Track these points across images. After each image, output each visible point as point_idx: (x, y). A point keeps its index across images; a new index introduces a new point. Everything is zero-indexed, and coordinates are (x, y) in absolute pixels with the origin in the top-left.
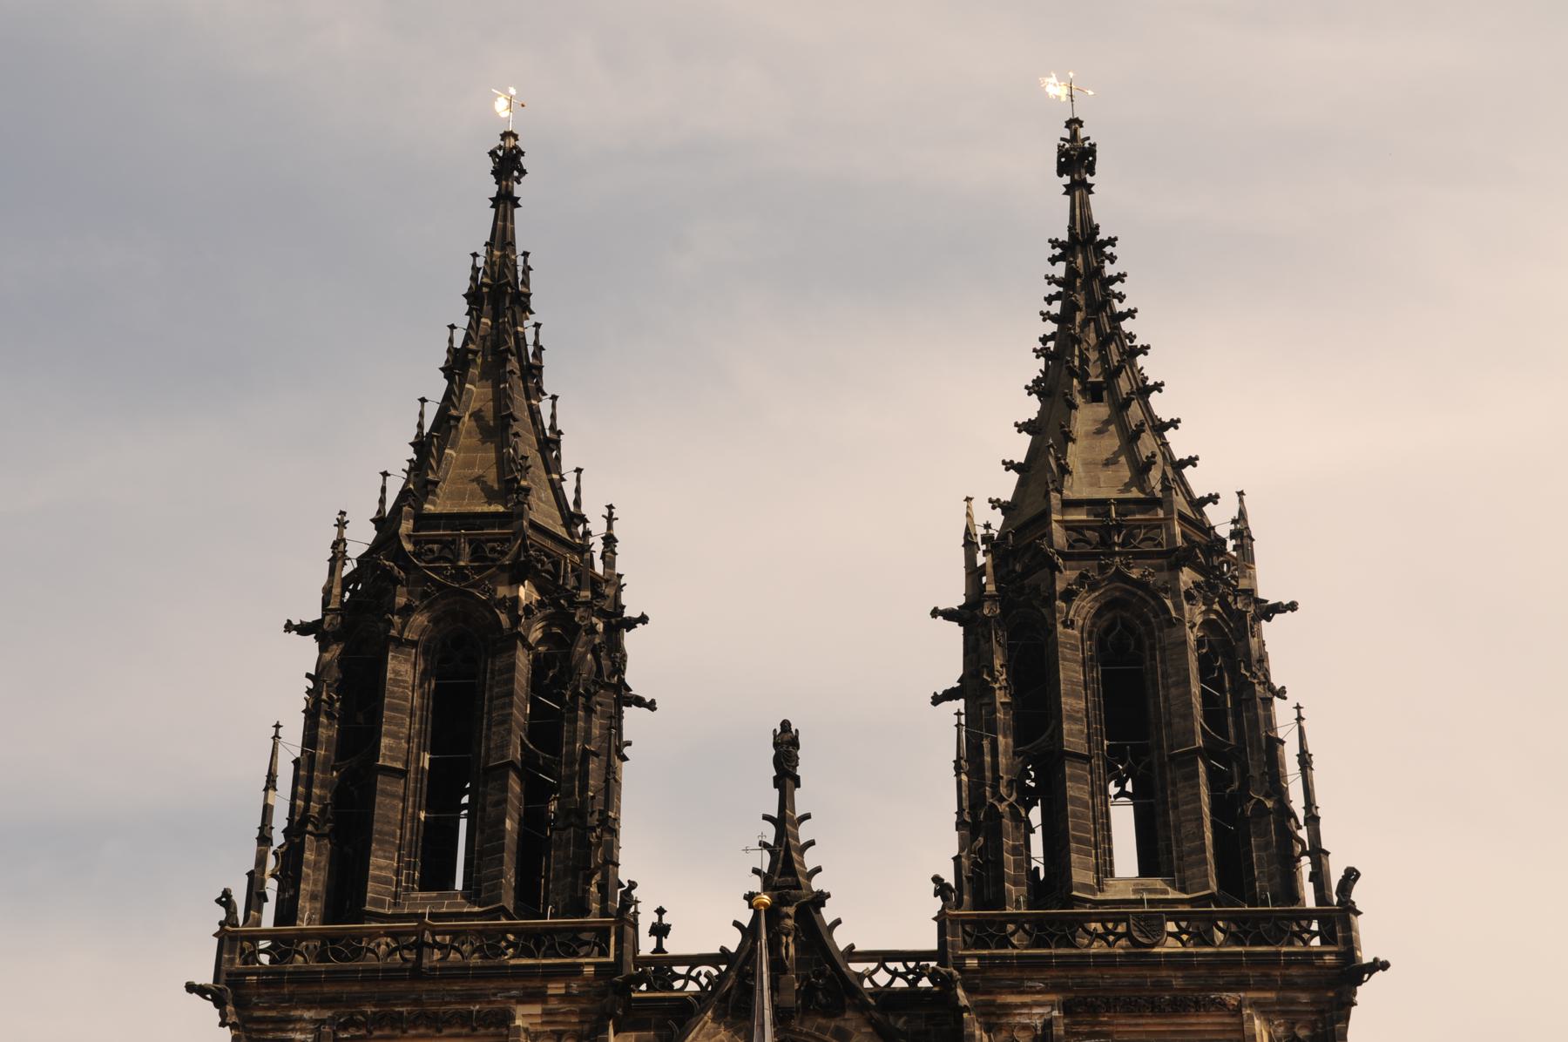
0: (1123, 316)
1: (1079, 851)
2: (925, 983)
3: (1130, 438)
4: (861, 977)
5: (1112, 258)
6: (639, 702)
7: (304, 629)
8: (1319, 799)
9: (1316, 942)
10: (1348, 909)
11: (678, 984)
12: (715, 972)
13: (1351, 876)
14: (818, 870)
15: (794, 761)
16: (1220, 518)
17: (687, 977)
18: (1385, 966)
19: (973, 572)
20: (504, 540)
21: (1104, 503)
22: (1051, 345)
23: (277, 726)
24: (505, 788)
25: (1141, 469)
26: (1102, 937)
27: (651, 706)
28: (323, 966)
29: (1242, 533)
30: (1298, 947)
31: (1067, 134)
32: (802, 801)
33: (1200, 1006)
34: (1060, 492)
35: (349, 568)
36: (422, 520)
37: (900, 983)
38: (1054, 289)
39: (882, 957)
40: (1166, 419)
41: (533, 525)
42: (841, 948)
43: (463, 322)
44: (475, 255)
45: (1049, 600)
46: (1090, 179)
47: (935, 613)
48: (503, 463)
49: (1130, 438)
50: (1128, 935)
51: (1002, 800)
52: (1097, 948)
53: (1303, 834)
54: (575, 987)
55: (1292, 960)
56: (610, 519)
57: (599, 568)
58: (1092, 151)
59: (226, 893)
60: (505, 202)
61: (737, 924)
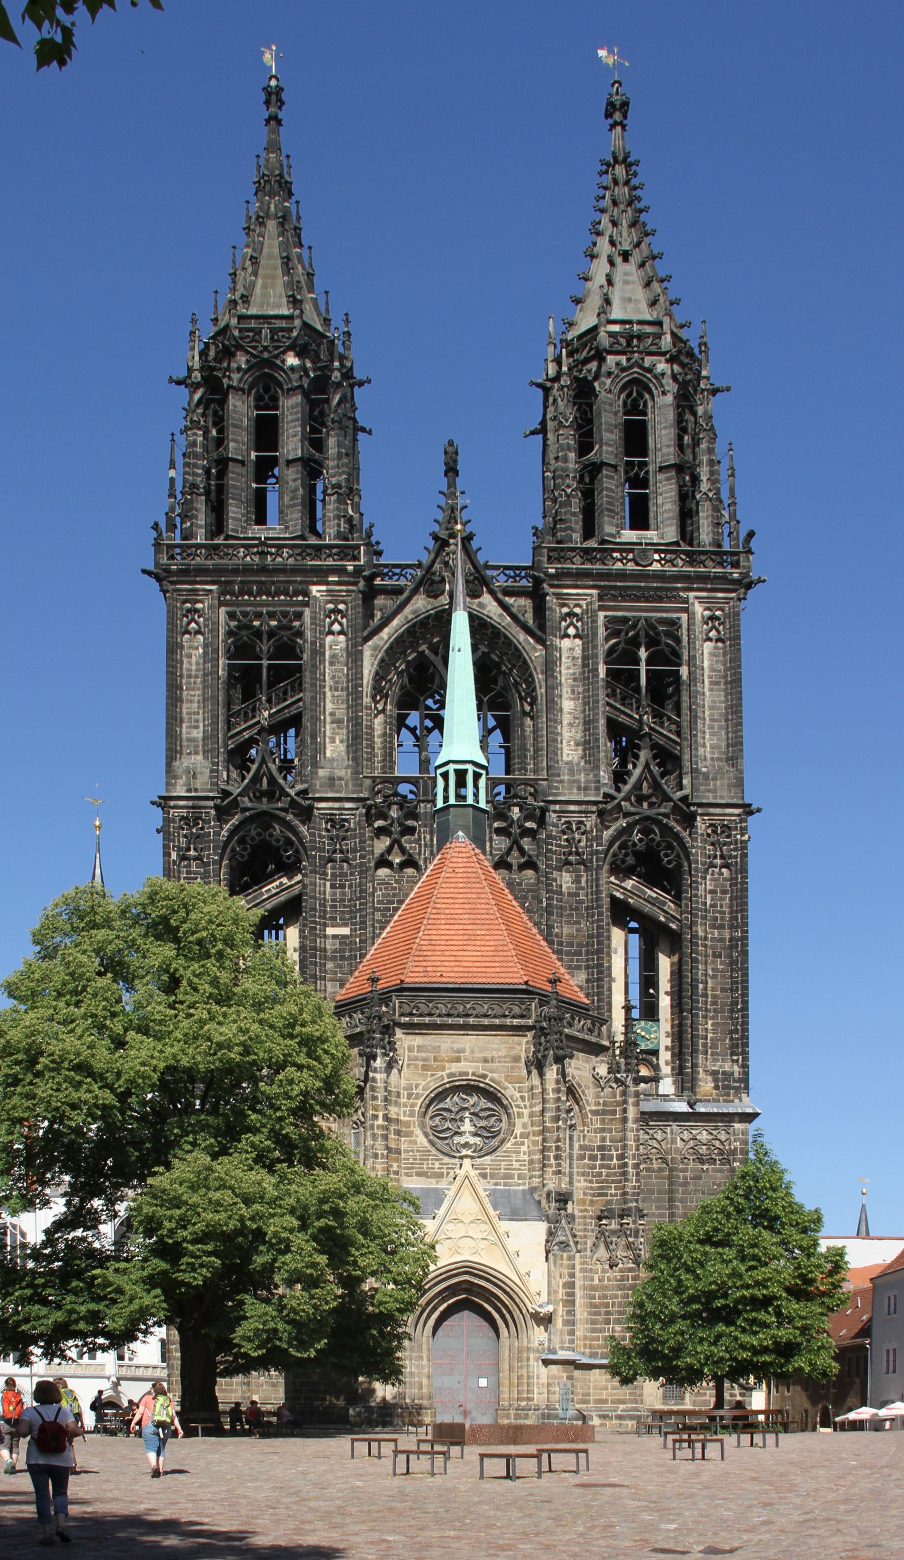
15: (455, 461)
44: (258, 156)
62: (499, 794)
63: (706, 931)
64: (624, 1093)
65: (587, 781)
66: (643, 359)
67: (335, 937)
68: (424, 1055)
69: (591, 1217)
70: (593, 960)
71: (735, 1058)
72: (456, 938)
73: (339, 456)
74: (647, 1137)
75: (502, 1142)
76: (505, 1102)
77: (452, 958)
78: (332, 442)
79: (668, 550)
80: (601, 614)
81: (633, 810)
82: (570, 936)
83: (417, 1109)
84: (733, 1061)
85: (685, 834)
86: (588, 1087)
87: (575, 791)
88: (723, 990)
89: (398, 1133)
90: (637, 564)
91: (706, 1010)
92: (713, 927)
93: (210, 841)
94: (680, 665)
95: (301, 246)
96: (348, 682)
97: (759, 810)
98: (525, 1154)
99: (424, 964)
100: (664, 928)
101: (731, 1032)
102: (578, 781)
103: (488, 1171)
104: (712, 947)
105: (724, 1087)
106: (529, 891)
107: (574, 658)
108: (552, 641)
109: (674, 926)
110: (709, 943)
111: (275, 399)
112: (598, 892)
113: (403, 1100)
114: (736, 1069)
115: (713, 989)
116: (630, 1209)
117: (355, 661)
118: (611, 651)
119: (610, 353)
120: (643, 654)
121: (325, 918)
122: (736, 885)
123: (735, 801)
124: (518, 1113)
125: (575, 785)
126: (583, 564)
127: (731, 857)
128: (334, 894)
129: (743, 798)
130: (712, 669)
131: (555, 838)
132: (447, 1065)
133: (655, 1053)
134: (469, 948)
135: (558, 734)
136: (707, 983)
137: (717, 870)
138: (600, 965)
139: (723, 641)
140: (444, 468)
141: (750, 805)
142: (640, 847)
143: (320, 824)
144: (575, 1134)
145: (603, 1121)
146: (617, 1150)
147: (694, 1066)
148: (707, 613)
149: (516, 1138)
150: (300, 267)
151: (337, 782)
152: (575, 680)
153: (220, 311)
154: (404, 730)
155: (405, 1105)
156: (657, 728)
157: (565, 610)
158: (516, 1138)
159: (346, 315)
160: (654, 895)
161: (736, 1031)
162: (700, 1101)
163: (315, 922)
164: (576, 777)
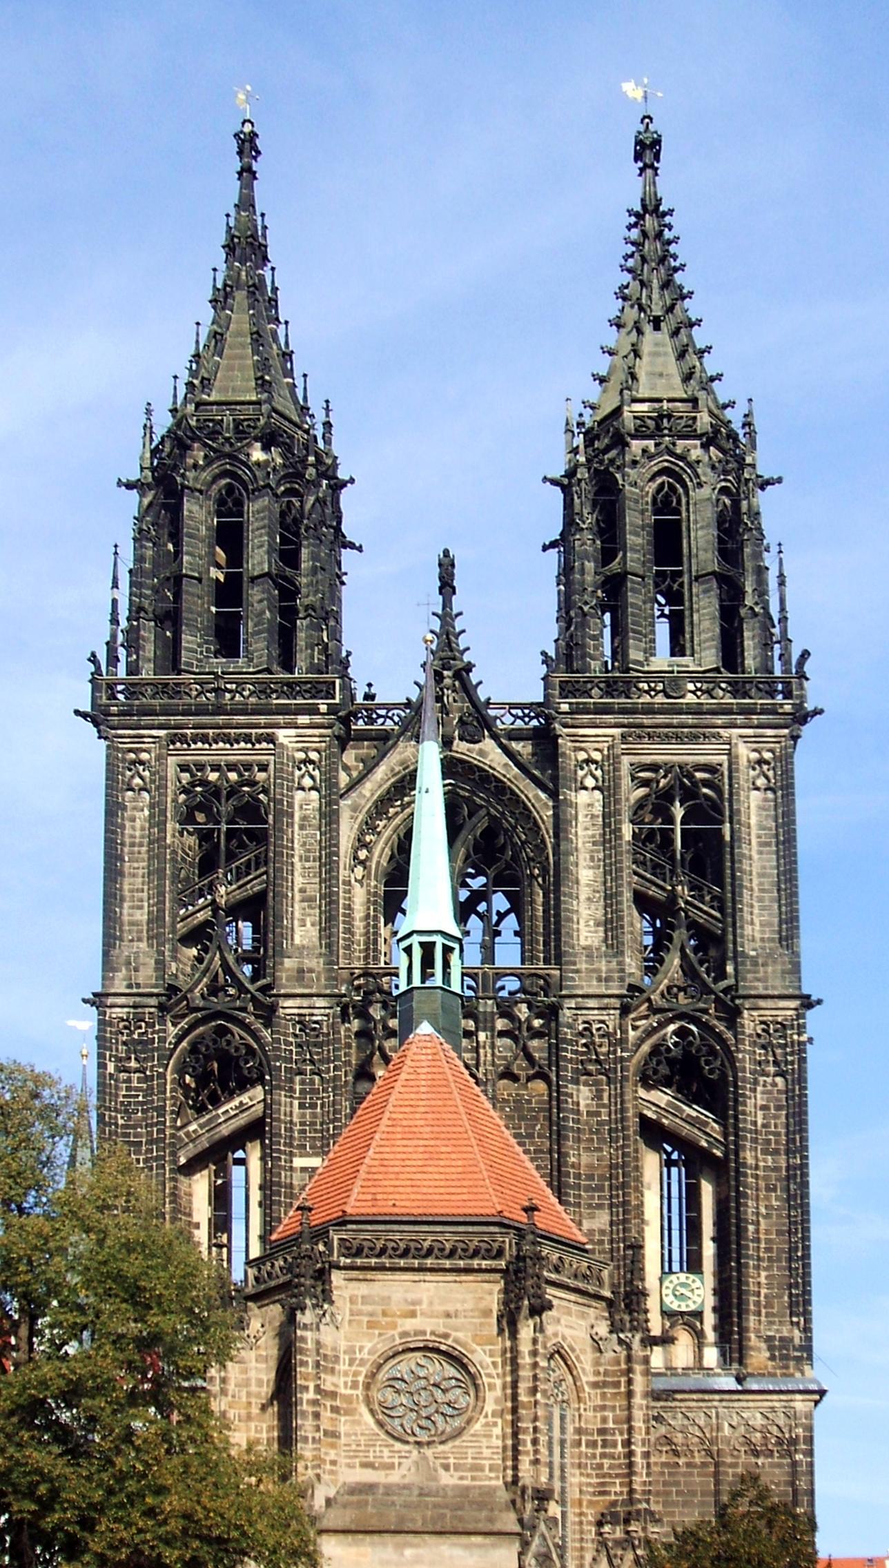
1: (634, 639)
5: (670, 227)
9: (780, 696)
11: (380, 721)
12: (403, 714)
14: (468, 649)
16: (735, 417)
17: (386, 717)
23: (116, 546)
26: (647, 692)
32: (457, 603)
42: (483, 699)
47: (545, 479)
50: (663, 691)
51: (586, 603)
54: (318, 719)
62: (503, 988)
63: (757, 1158)
64: (629, 1359)
65: (609, 971)
66: (674, 444)
67: (304, 1169)
68: (369, 1308)
69: (589, 1523)
70: (618, 1196)
71: (795, 1319)
72: (415, 1156)
73: (314, 571)
74: (686, 1422)
75: (469, 1422)
76: (472, 1370)
77: (409, 1183)
78: (304, 553)
79: (707, 680)
80: (626, 760)
82: (590, 1166)
83: (361, 1379)
84: (792, 1323)
85: (729, 1035)
86: (583, 1351)
87: (595, 983)
88: (779, 1233)
89: (335, 1410)
90: (668, 697)
91: (759, 1259)
92: (765, 1152)
93: (153, 1050)
94: (722, 822)
95: (277, 320)
96: (321, 850)
97: (819, 1002)
99: (373, 1190)
100: (706, 1155)
101: (790, 1286)
102: (598, 971)
104: (766, 1178)
105: (783, 1357)
106: (541, 1110)
107: (593, 816)
108: (564, 794)
109: (719, 1153)
110: (761, 1173)
111: (239, 503)
112: (623, 1110)
113: (342, 1367)
114: (797, 1334)
115: (767, 1232)
116: (638, 1511)
117: (329, 824)
118: (640, 805)
119: (634, 437)
120: (678, 811)
121: (291, 1145)
122: (793, 1097)
123: (791, 991)
124: (489, 1385)
125: (595, 975)
126: (601, 697)
128: (303, 1115)
129: (800, 988)
130: (761, 828)
131: (570, 1042)
132: (400, 1321)
133: (698, 1315)
134: (430, 1169)
135: (572, 911)
136: (758, 1223)
138: (625, 1203)
139: (774, 791)
140: (439, 584)
141: (808, 997)
142: (676, 1052)
143: (286, 1027)
144: (569, 1413)
145: (604, 1395)
146: (621, 1434)
147: (742, 1331)
148: (754, 756)
150: (275, 347)
151: (307, 975)
152: (594, 843)
153: (179, 401)
155: (346, 1374)
156: (696, 902)
157: (582, 756)
159: (327, 401)
160: (694, 1114)
161: (796, 1285)
162: (752, 1375)
163: (279, 1151)
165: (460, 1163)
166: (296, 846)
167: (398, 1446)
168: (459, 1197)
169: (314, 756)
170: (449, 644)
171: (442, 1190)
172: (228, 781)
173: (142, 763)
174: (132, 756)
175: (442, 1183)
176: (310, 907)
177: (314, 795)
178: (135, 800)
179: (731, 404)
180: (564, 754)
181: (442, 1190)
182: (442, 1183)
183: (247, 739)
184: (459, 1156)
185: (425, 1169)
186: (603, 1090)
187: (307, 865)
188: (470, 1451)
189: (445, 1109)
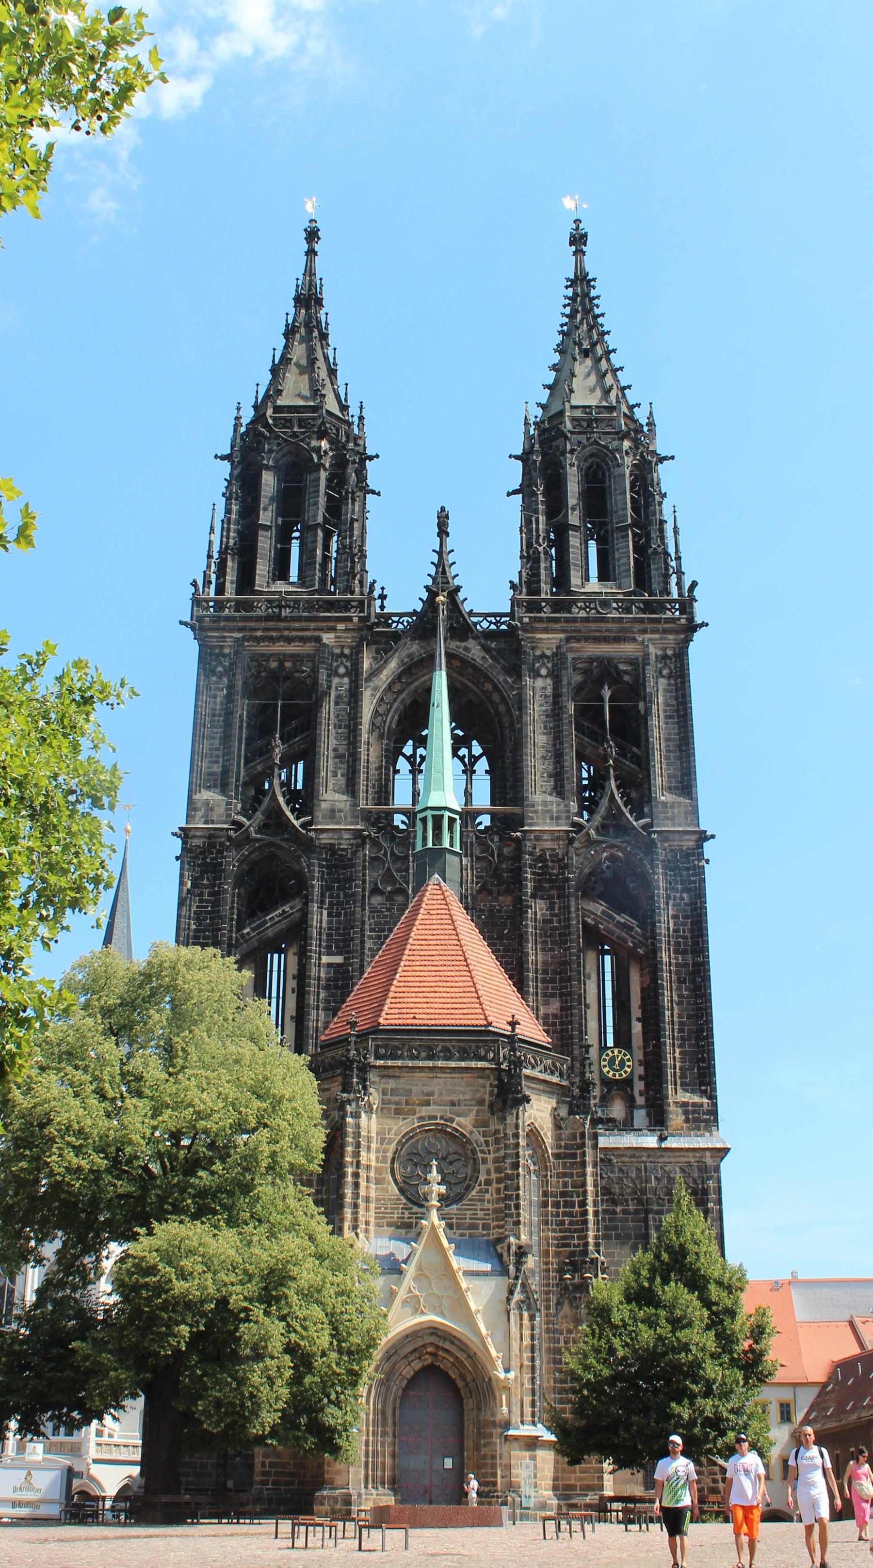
0: (598, 316)
2: (504, 627)
3: (602, 376)
4: (475, 624)
6: (373, 492)
7: (223, 458)
8: (681, 548)
9: (677, 613)
10: (693, 599)
11: (394, 625)
13: (694, 585)
16: (641, 415)
17: (398, 622)
18: (707, 625)
19: (528, 437)
20: (314, 419)
21: (589, 407)
22: (565, 328)
24: (316, 535)
25: (607, 392)
26: (584, 609)
27: (379, 494)
28: (237, 614)
29: (651, 424)
30: (669, 614)
31: (574, 226)
32: (450, 543)
33: (625, 640)
34: (569, 402)
35: (243, 429)
36: (278, 409)
37: (493, 627)
38: (567, 301)
39: (486, 616)
40: (617, 366)
41: (327, 411)
43: (292, 311)
45: (564, 453)
46: (584, 249)
48: (313, 382)
49: (602, 376)
52: (582, 614)
53: (673, 564)
54: (350, 626)
55: (668, 621)
56: (361, 408)
57: (356, 431)
58: (585, 236)
59: (195, 581)
60: (311, 253)
61: (420, 599)
62: (480, 823)
65: (558, 812)
72: (429, 979)
75: (468, 1189)
81: (600, 838)
98: (489, 1202)
102: (551, 811)
103: (454, 1220)
113: (373, 1146)
127: (690, 882)
137: (678, 895)
142: (608, 874)
149: (480, 1185)
154: (401, 758)
158: (480, 1185)
164: (549, 807)
165: (461, 984)
166: (332, 716)
167: (415, 1209)
168: (461, 1011)
169: (347, 651)
170: (444, 572)
171: (449, 1006)
172: (284, 668)
173: (224, 656)
174: (217, 651)
175: (449, 1000)
176: (341, 762)
177: (346, 680)
178: (216, 683)
179: (638, 405)
180: (525, 652)
181: (449, 1006)
182: (449, 1000)
183: (302, 639)
184: (461, 979)
185: (436, 989)
186: (554, 903)
187: (340, 731)
188: (468, 1212)
189: (451, 942)
